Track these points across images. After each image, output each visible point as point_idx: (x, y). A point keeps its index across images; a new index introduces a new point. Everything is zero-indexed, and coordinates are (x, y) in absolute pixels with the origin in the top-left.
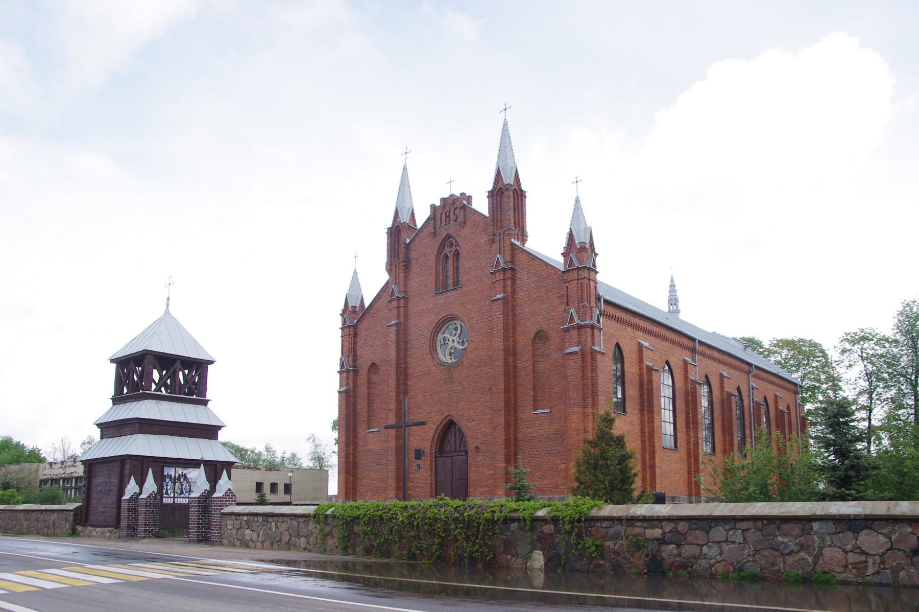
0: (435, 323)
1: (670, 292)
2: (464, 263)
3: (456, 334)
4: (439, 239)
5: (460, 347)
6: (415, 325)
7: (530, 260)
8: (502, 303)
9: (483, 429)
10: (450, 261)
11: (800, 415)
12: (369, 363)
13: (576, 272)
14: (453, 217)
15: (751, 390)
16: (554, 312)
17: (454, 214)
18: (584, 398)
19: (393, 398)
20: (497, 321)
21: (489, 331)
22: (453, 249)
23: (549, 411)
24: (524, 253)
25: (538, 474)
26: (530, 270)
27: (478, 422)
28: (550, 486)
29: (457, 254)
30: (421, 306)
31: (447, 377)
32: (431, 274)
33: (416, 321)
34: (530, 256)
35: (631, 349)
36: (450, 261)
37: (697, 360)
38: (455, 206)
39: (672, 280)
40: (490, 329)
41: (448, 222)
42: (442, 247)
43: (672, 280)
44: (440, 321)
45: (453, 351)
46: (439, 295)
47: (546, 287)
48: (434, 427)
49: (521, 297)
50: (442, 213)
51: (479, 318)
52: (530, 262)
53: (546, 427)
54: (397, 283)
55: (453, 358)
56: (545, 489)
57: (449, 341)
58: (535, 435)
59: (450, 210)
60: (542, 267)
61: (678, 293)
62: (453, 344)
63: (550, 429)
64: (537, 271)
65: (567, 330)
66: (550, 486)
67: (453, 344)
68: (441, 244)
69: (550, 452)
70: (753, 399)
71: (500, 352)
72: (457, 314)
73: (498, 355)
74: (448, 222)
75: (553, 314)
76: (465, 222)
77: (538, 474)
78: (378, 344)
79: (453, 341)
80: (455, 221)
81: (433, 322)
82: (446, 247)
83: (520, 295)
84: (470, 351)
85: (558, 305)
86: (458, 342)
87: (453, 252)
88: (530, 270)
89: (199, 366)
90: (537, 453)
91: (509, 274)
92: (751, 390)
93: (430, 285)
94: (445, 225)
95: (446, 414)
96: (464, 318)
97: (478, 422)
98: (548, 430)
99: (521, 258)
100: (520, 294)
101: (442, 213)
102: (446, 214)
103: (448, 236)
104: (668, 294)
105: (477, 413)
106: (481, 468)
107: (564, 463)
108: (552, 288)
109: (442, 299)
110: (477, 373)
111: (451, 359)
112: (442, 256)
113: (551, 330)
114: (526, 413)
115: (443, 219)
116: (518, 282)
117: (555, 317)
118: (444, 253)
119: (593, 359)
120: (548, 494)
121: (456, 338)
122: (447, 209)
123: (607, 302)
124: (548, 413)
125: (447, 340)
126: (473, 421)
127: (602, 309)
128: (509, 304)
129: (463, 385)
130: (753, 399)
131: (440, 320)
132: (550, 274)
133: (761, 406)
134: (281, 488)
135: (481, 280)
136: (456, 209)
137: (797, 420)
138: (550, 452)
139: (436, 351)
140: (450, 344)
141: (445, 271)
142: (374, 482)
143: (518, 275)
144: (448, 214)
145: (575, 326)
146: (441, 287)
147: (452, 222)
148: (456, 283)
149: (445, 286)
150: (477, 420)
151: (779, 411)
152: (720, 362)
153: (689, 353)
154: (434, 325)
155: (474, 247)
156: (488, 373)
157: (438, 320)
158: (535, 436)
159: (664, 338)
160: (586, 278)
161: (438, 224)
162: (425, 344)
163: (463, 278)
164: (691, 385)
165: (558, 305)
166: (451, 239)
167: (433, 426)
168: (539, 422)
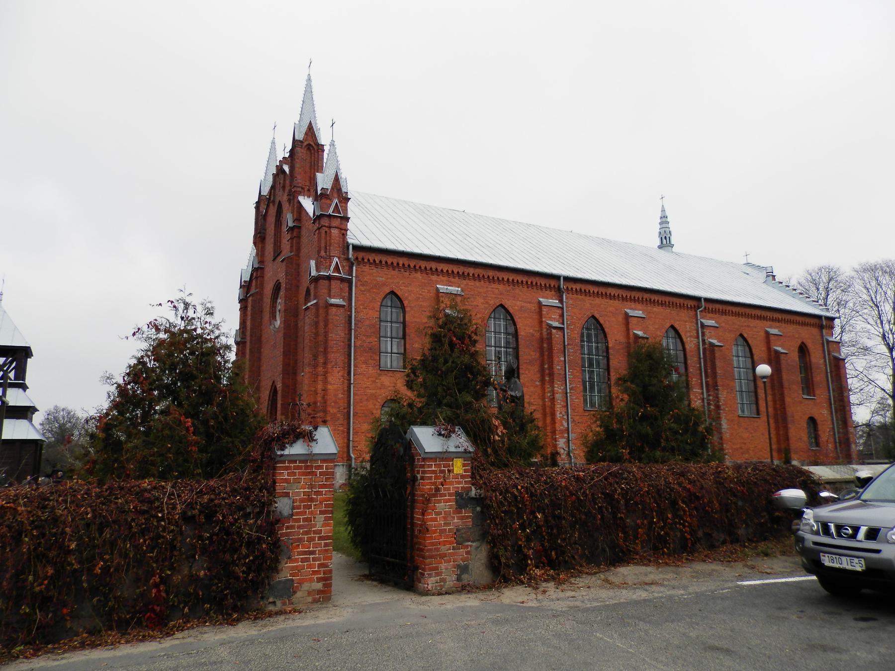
1: (661, 223)
11: (829, 354)
15: (700, 329)
18: (315, 357)
35: (421, 296)
39: (663, 211)
43: (663, 211)
48: (268, 392)
61: (670, 225)
70: (704, 341)
92: (700, 329)
104: (659, 227)
119: (327, 313)
123: (357, 248)
130: (704, 341)
133: (716, 348)
137: (825, 361)
139: (275, 316)
151: (773, 353)
152: (624, 299)
153: (553, 292)
159: (500, 281)
160: (325, 226)
164: (547, 329)
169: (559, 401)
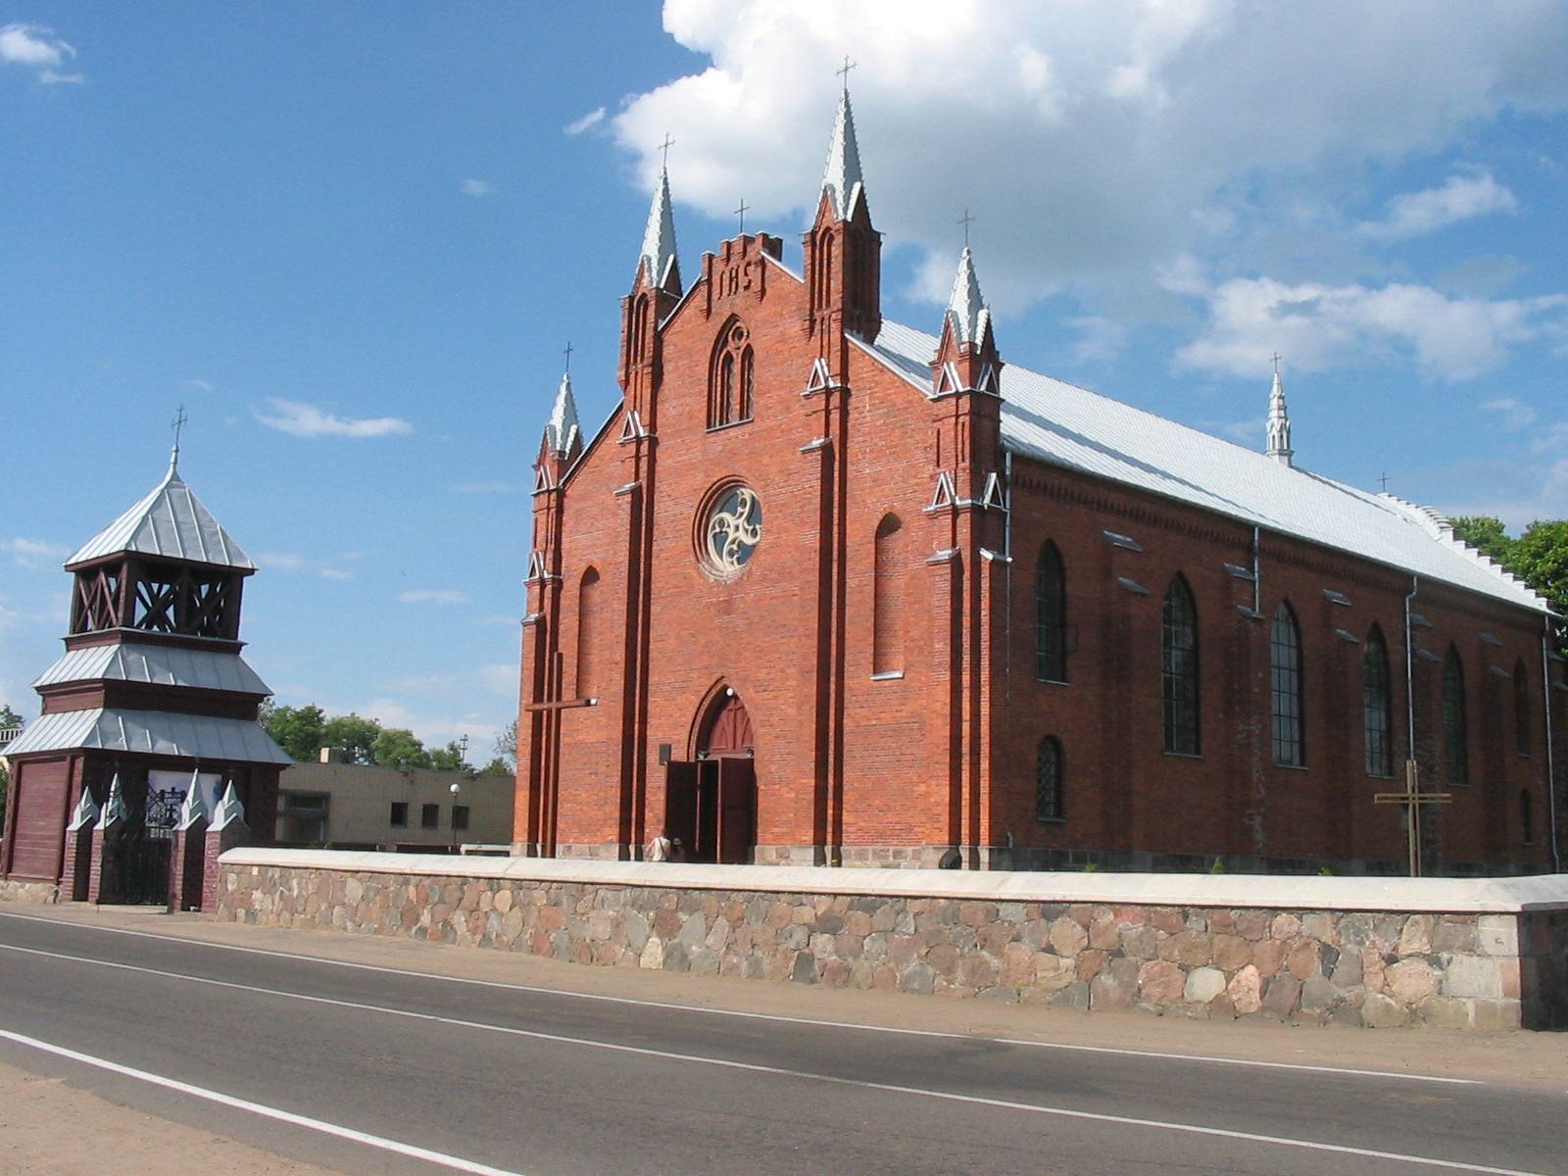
0: (704, 491)
2: (760, 374)
3: (742, 514)
4: (718, 321)
5: (749, 541)
6: (669, 493)
8: (820, 457)
10: (736, 368)
12: (583, 567)
14: (743, 281)
16: (915, 476)
17: (746, 274)
19: (620, 640)
22: (743, 343)
23: (901, 676)
24: (867, 357)
25: (877, 802)
27: (774, 693)
28: (897, 827)
29: (749, 352)
30: (680, 456)
31: (722, 599)
34: (876, 364)
36: (736, 368)
37: (1256, 569)
41: (733, 290)
42: (721, 341)
44: (714, 488)
45: (735, 547)
46: (713, 434)
51: (781, 485)
52: (875, 376)
54: (638, 408)
55: (735, 563)
56: (889, 833)
57: (729, 526)
58: (874, 722)
59: (738, 267)
60: (897, 387)
63: (901, 711)
64: (889, 395)
65: (933, 516)
66: (897, 827)
67: (737, 534)
68: (721, 333)
69: (902, 758)
74: (733, 290)
76: (763, 291)
77: (877, 802)
80: (747, 288)
81: (701, 489)
82: (730, 338)
84: (765, 551)
85: (921, 465)
86: (747, 531)
87: (742, 349)
89: (229, 580)
90: (878, 759)
94: (729, 295)
95: (718, 676)
100: (856, 440)
103: (733, 318)
105: (772, 676)
106: (777, 787)
108: (913, 430)
109: (719, 441)
111: (732, 563)
112: (722, 356)
114: (859, 677)
115: (726, 283)
117: (916, 488)
121: (741, 521)
122: (733, 264)
124: (900, 680)
125: (726, 525)
127: (1008, 473)
128: (833, 461)
129: (748, 618)
134: (415, 815)
135: (788, 409)
136: (749, 264)
138: (902, 758)
141: (726, 386)
145: (947, 508)
146: (716, 415)
147: (741, 290)
148: (743, 413)
149: (724, 418)
150: (771, 688)
154: (702, 495)
155: (778, 342)
156: (796, 595)
157: (711, 484)
163: (758, 401)
166: (738, 324)
167: (693, 697)
169: (1256, 750)
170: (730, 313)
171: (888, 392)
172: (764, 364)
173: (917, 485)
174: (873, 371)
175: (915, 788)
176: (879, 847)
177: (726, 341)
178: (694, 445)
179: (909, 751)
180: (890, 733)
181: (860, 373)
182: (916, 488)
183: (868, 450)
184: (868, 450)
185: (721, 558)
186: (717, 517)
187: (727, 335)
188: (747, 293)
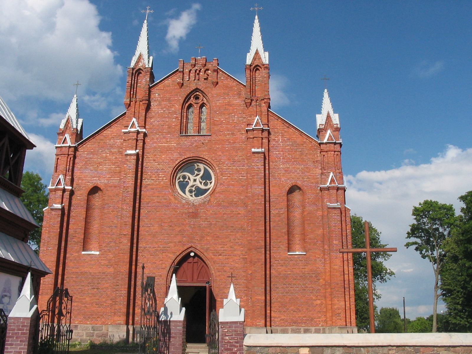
0: (179, 161)
5: (203, 187)
7: (286, 127)
9: (232, 263)
12: (91, 186)
13: (333, 145)
16: (308, 172)
19: (127, 223)
20: (258, 171)
21: (241, 177)
25: (293, 308)
26: (285, 135)
27: (227, 257)
28: (304, 318)
32: (177, 117)
33: (155, 155)
38: (206, 67)
40: (242, 176)
42: (188, 98)
45: (194, 189)
47: (301, 151)
49: (276, 155)
50: (191, 70)
52: (284, 128)
53: (301, 267)
55: (193, 196)
57: (189, 179)
59: (201, 70)
62: (195, 183)
63: (305, 269)
65: (328, 189)
67: (195, 183)
71: (260, 197)
72: (205, 157)
73: (258, 199)
75: (307, 174)
78: (105, 169)
79: (195, 180)
81: (176, 160)
83: (274, 153)
84: (219, 192)
85: (313, 168)
88: (285, 135)
90: (291, 289)
91: (265, 134)
93: (174, 127)
94: (195, 80)
96: (212, 162)
97: (227, 257)
98: (303, 270)
99: (276, 124)
101: (191, 70)
102: (196, 71)
107: (319, 299)
108: (306, 154)
109: (186, 142)
110: (227, 213)
111: (192, 196)
113: (306, 186)
116: (272, 143)
117: (309, 177)
118: (189, 103)
120: (303, 325)
126: (220, 255)
129: (209, 222)
131: (184, 159)
132: (305, 142)
140: (191, 183)
142: (87, 306)
143: (272, 137)
144: (198, 72)
150: (224, 254)
154: (177, 162)
158: (289, 274)
161: (187, 78)
162: (164, 178)
165: (313, 168)
166: (198, 93)
167: (171, 255)
168: (292, 262)
170: (195, 88)
171: (292, 136)
172: (217, 112)
173: (310, 175)
174: (283, 126)
175: (314, 302)
176: (294, 327)
177: (190, 98)
178: (172, 140)
179: (310, 286)
180: (298, 278)
181: (276, 126)
182: (309, 177)
183: (281, 158)
184: (281, 158)
185: (185, 194)
186: (181, 174)
187: (191, 96)
188: (205, 81)
